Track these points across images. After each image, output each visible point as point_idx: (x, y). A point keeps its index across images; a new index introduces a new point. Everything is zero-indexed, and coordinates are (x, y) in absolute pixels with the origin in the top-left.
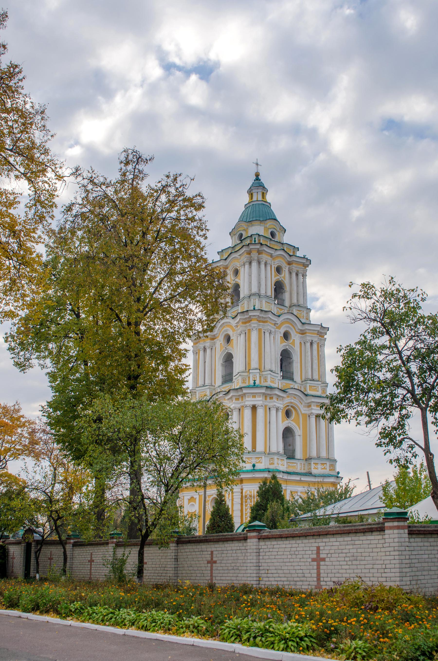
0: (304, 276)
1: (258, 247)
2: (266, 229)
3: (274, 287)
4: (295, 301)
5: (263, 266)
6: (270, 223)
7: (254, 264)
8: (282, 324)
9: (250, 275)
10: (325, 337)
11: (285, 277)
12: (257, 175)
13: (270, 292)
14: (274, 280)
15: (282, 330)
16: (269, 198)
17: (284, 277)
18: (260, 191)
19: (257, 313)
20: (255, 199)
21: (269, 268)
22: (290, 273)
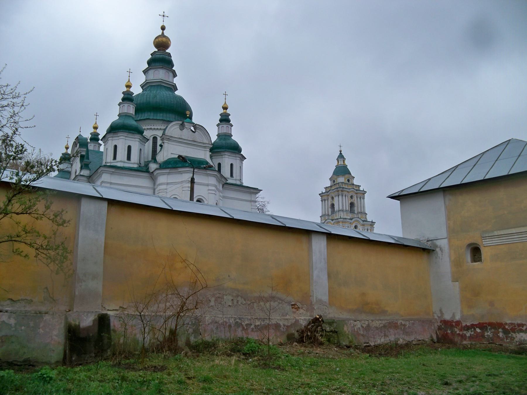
0: (364, 198)
1: (341, 189)
2: (345, 179)
3: (349, 205)
4: (359, 211)
5: (344, 197)
6: (347, 176)
7: (340, 197)
8: (354, 222)
9: (339, 201)
10: (374, 226)
11: (355, 200)
12: (341, 151)
13: (348, 208)
14: (349, 202)
15: (354, 225)
16: (346, 162)
17: (354, 200)
18: (342, 159)
19: (342, 220)
20: (340, 163)
21: (347, 197)
22: (357, 198)
